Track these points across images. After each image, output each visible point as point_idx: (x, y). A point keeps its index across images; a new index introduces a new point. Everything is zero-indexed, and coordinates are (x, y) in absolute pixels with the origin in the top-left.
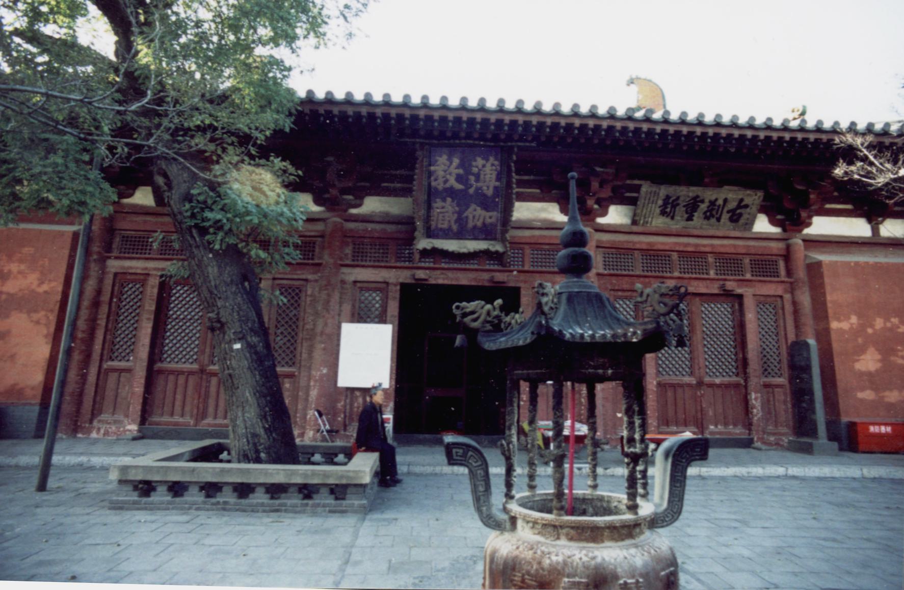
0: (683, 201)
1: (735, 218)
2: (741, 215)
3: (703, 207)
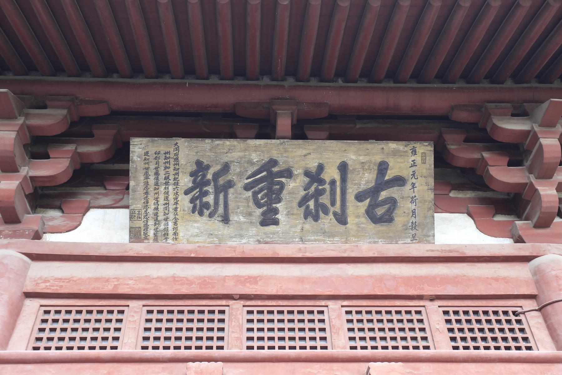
0: (240, 175)
1: (380, 211)
2: (392, 202)
3: (295, 186)
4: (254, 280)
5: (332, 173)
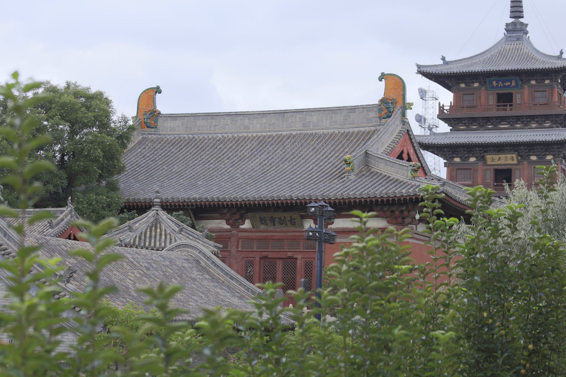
4: (273, 236)
5: (282, 218)
